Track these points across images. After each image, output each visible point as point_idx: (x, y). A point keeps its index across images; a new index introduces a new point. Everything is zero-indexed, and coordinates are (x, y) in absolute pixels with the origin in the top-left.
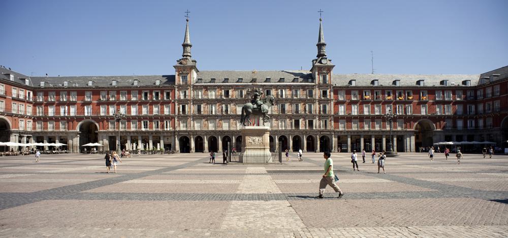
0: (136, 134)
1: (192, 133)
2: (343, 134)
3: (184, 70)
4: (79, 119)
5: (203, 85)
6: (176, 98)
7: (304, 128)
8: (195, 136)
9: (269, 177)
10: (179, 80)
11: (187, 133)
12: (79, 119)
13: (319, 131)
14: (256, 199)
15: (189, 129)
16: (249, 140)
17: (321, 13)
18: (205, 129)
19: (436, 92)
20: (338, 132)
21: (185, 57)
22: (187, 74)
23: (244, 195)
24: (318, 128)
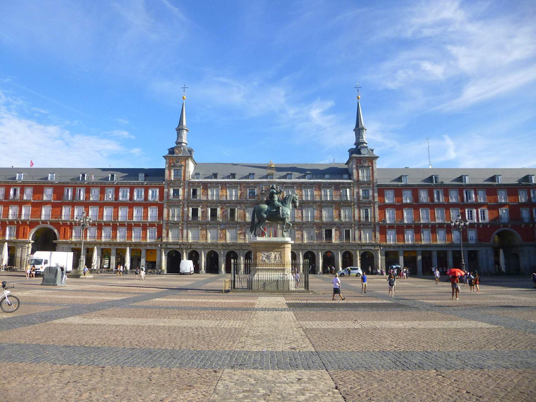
0: (108, 247)
1: (184, 247)
2: (392, 249)
3: (177, 162)
4: (32, 224)
5: (201, 182)
6: (165, 199)
7: (338, 242)
8: (189, 251)
9: (290, 315)
10: (170, 175)
11: (178, 247)
12: (32, 224)
13: (359, 245)
14: (267, 368)
15: (180, 241)
16: (261, 256)
17: (359, 89)
18: (202, 241)
19: (520, 192)
20: (385, 246)
21: (179, 145)
22: (181, 166)
23: (246, 353)
24: (358, 241)
